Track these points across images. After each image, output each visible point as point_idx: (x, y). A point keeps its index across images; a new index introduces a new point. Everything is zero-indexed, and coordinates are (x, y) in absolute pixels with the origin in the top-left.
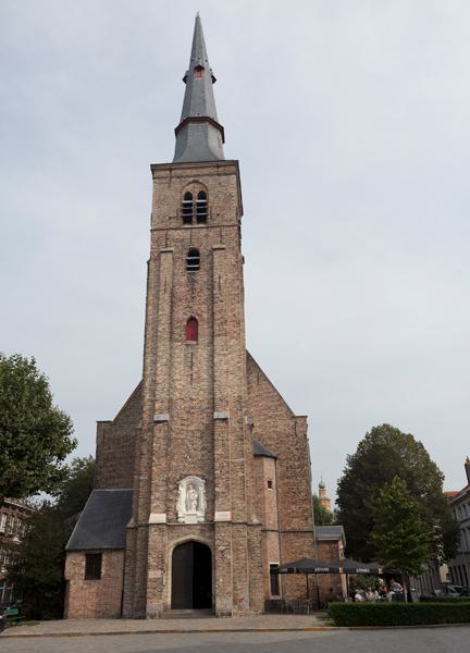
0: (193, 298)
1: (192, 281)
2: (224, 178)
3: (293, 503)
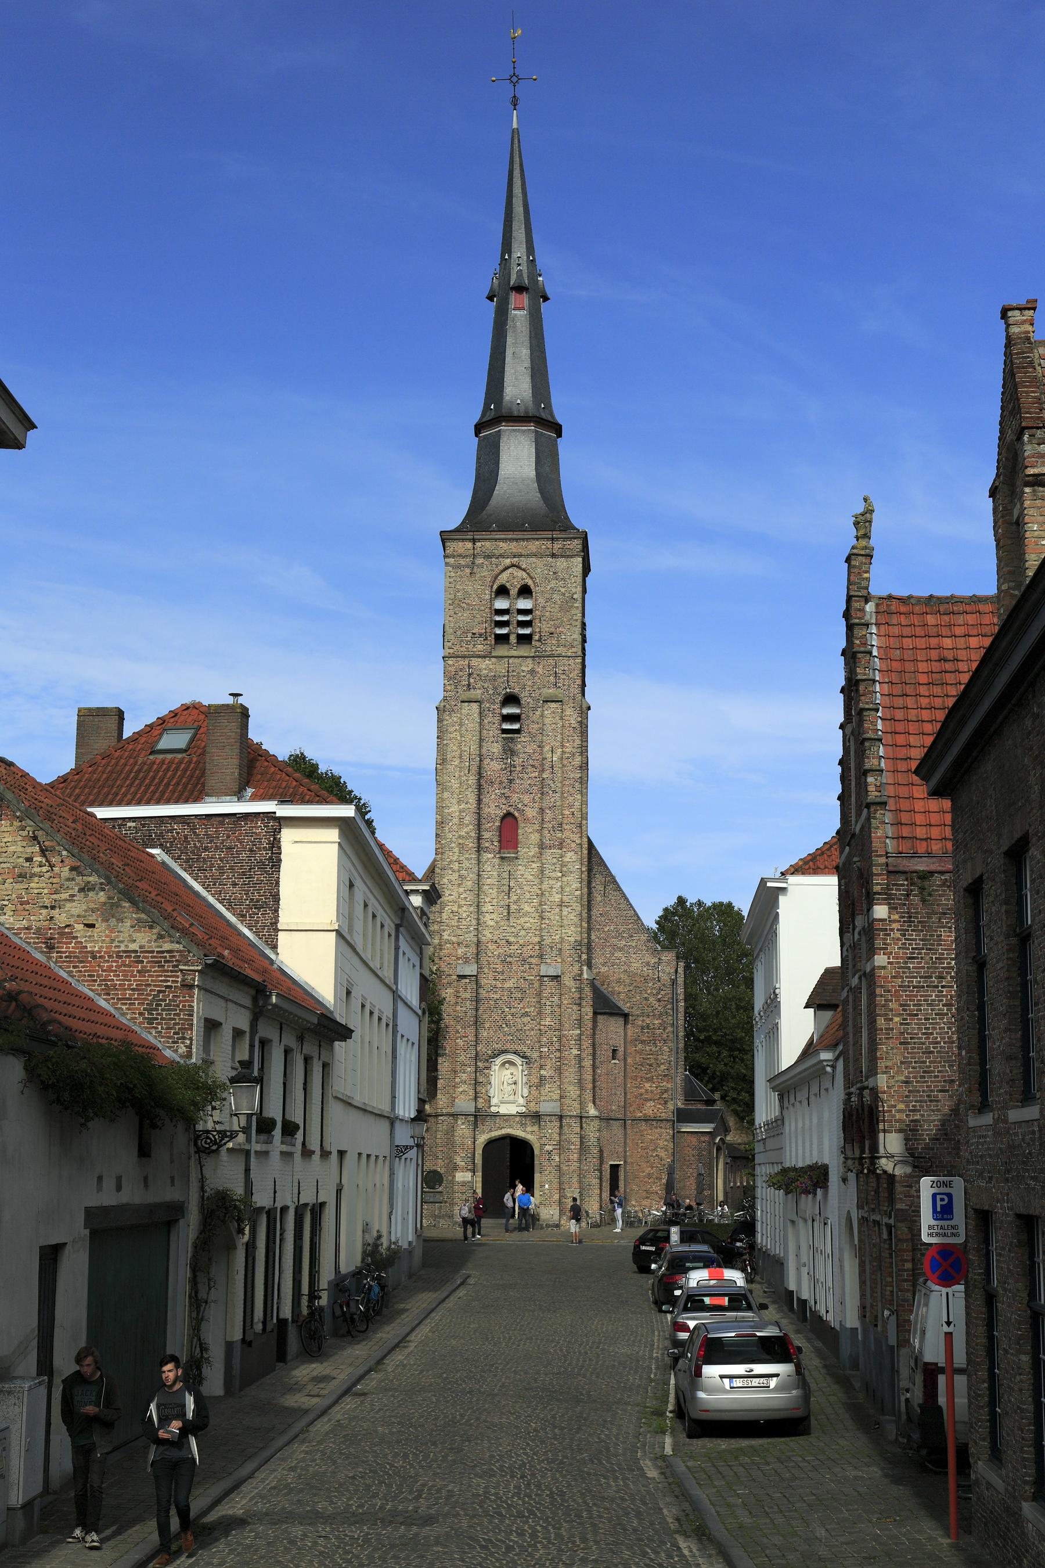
0: (511, 781)
1: (509, 752)
2: (561, 563)
3: (650, 1080)
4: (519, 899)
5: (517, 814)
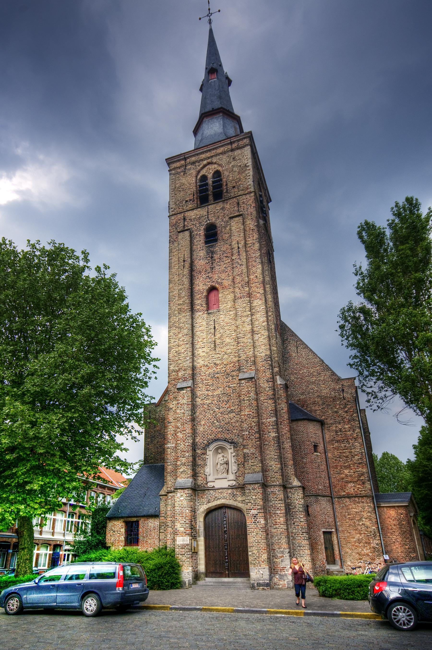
0: (212, 268)
4: (222, 336)
5: (217, 286)
